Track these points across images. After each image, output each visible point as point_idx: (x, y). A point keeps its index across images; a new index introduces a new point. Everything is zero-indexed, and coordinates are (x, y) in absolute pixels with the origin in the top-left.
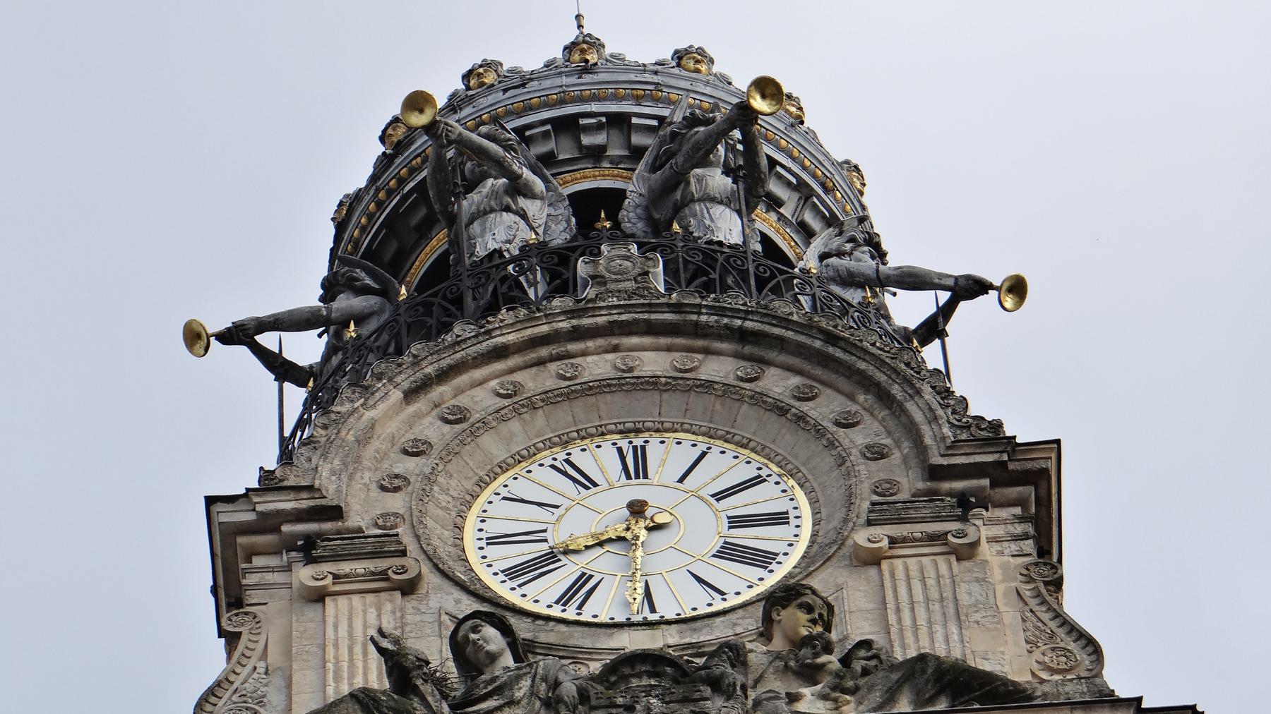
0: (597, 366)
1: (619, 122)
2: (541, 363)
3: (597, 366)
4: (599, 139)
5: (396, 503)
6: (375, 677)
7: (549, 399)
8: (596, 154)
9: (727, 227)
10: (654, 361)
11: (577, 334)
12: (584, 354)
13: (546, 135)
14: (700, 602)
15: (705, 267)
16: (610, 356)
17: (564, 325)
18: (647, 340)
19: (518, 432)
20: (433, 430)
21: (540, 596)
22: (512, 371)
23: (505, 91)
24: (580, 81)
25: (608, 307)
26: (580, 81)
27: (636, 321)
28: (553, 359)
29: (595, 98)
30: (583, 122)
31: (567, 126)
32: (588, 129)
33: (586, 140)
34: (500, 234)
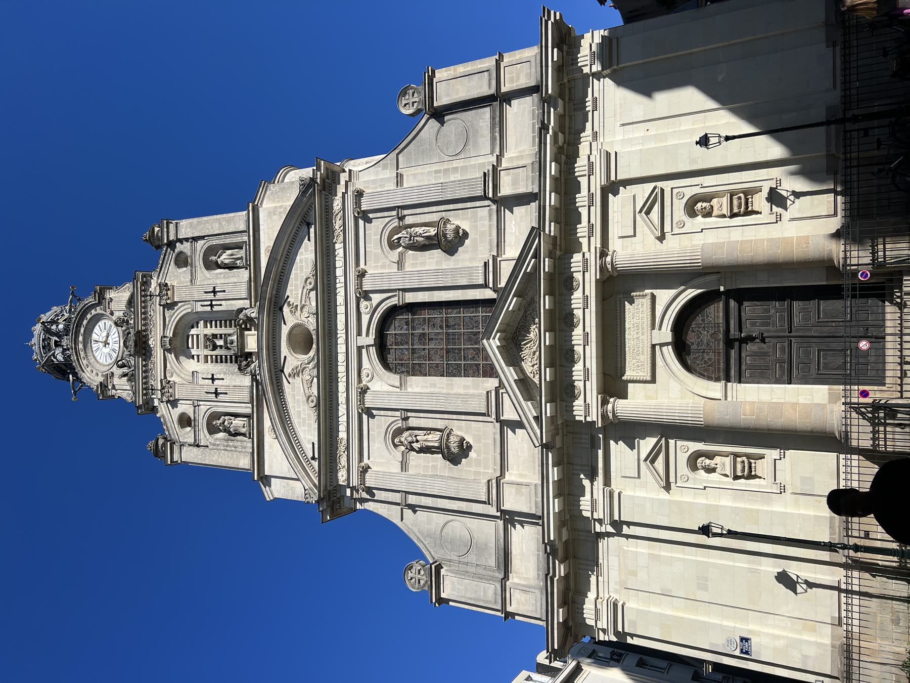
0: (81, 346)
1: (43, 340)
3: (81, 346)
5: (100, 374)
6: (126, 378)
7: (85, 352)
8: (49, 344)
9: (61, 327)
10: (81, 338)
11: (75, 348)
14: (117, 335)
15: (67, 330)
19: (91, 357)
20: (89, 369)
21: (115, 355)
31: (43, 347)
34: (60, 357)
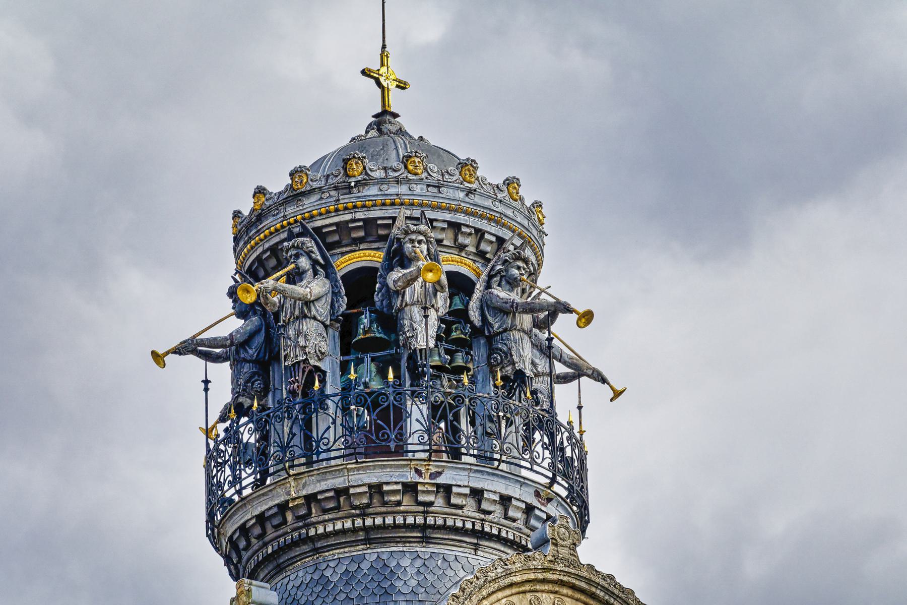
1: (480, 234)
2: (524, 592)
4: (467, 241)
12: (542, 591)
13: (443, 229)
16: (552, 596)
17: (540, 576)
18: (570, 592)
22: (512, 595)
23: (428, 186)
24: (467, 199)
25: (561, 571)
26: (467, 199)
27: (569, 582)
28: (530, 591)
29: (473, 214)
30: (464, 229)
32: (463, 233)
33: (461, 239)
